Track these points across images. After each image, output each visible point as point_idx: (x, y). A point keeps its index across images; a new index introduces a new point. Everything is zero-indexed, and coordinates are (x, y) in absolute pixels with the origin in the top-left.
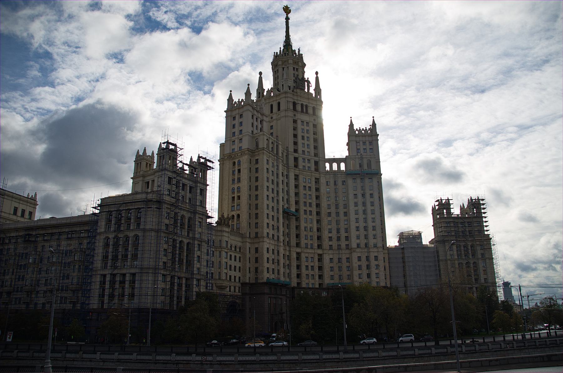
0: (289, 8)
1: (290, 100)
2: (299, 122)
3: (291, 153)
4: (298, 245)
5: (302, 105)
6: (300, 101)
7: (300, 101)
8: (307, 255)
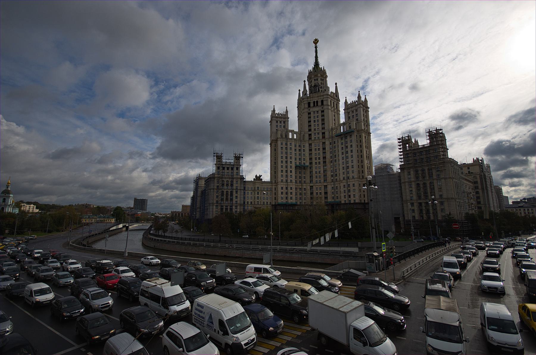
0: (317, 39)
1: (305, 102)
2: (312, 113)
3: (307, 133)
4: (311, 181)
5: (314, 102)
8: (317, 187)
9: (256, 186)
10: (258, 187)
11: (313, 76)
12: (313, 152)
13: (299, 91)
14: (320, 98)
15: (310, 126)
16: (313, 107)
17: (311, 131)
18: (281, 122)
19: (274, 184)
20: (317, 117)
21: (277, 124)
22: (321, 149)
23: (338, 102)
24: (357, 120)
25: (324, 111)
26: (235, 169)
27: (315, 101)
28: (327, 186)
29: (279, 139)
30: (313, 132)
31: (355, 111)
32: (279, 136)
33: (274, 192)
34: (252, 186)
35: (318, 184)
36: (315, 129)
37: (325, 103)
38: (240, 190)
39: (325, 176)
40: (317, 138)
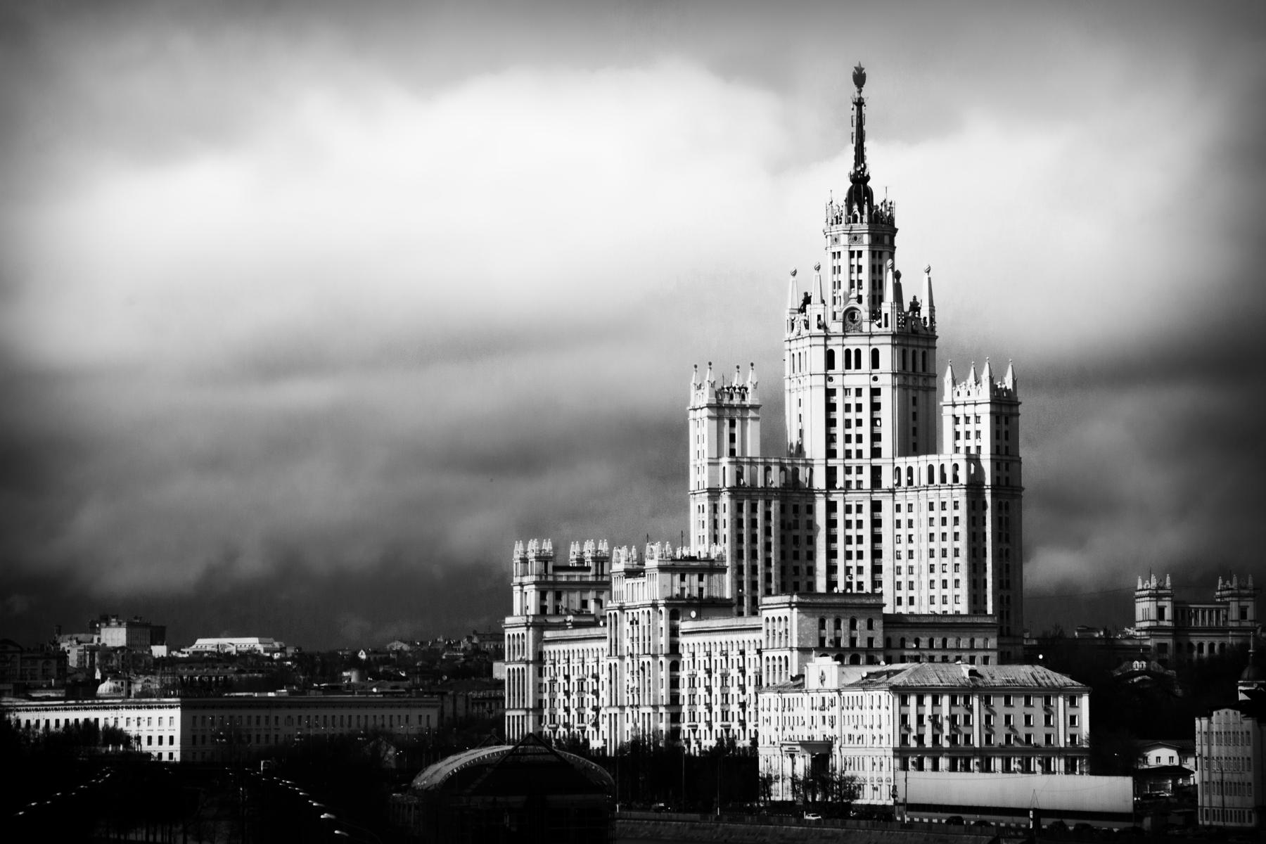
2: (840, 392)
5: (848, 352)
11: (844, 239)
14: (866, 340)
15: (830, 438)
23: (931, 344)
27: (853, 350)
31: (972, 420)
40: (854, 486)
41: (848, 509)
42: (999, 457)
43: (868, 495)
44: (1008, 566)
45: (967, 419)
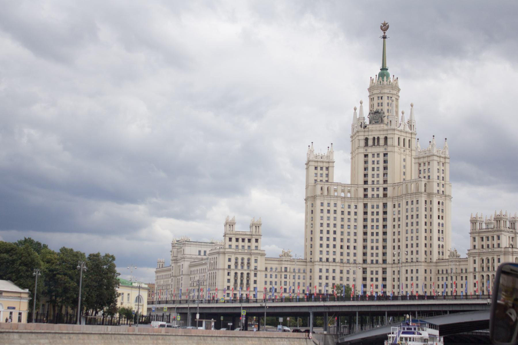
2: (370, 156)
6: (372, 135)
7: (372, 135)
8: (372, 269)
9: (283, 266)
10: (286, 268)
12: (369, 217)
13: (355, 109)
14: (382, 133)
15: (366, 175)
16: (372, 146)
17: (367, 184)
18: (322, 168)
19: (311, 264)
20: (378, 163)
21: (316, 171)
22: (381, 213)
24: (429, 176)
25: (387, 154)
26: (253, 240)
27: (376, 138)
28: (386, 268)
29: (318, 198)
30: (370, 186)
31: (427, 164)
32: (319, 192)
33: (308, 274)
34: (277, 266)
35: (372, 266)
36: (373, 181)
37: (389, 142)
38: (260, 271)
39: (384, 254)
40: (375, 196)
41: (373, 207)
42: (438, 181)
43: (382, 200)
44: (442, 231)
45: (424, 164)
